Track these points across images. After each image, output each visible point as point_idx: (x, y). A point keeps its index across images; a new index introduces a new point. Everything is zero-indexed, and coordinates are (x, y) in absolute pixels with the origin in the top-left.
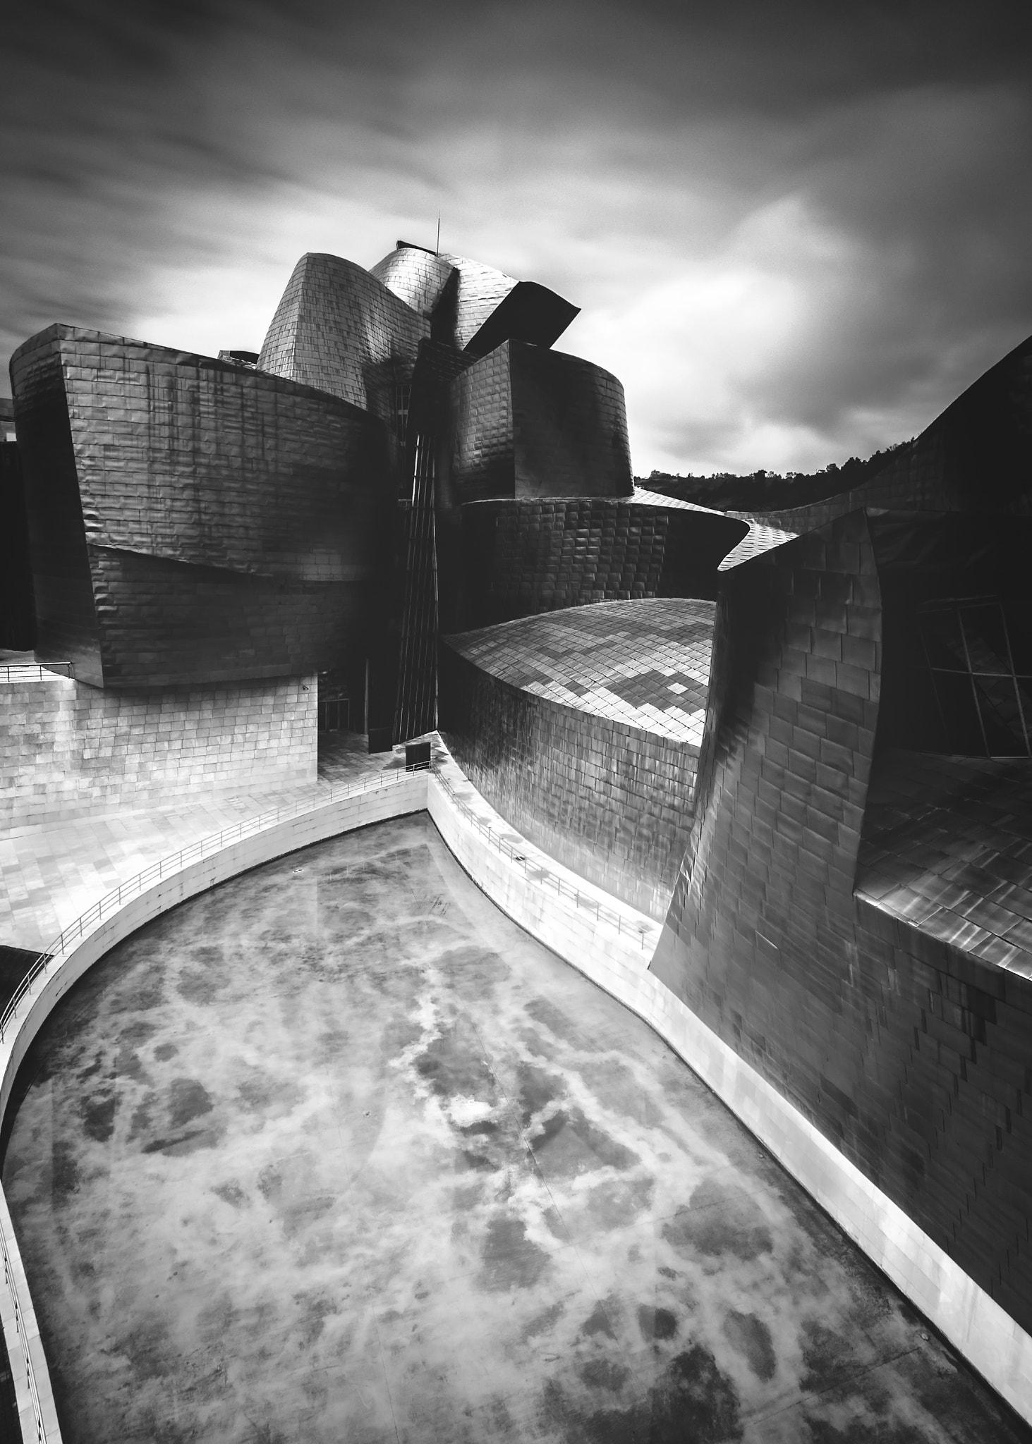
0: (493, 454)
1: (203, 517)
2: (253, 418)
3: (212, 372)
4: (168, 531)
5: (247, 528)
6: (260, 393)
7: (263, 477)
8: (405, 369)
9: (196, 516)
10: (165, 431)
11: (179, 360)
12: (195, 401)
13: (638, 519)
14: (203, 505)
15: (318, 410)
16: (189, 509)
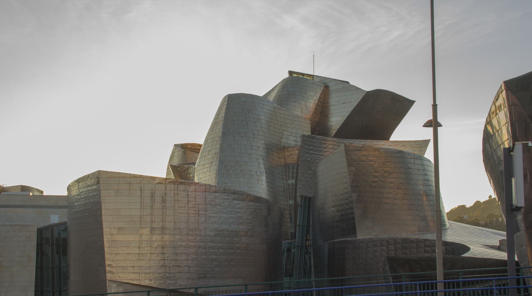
0: (342, 210)
1: (166, 262)
2: (193, 207)
3: (173, 186)
4: (148, 271)
5: (189, 267)
6: (197, 194)
7: (199, 238)
8: (292, 155)
9: (162, 262)
10: (148, 219)
11: (157, 182)
12: (164, 201)
13: (428, 249)
14: (166, 256)
15: (229, 199)
16: (160, 258)
